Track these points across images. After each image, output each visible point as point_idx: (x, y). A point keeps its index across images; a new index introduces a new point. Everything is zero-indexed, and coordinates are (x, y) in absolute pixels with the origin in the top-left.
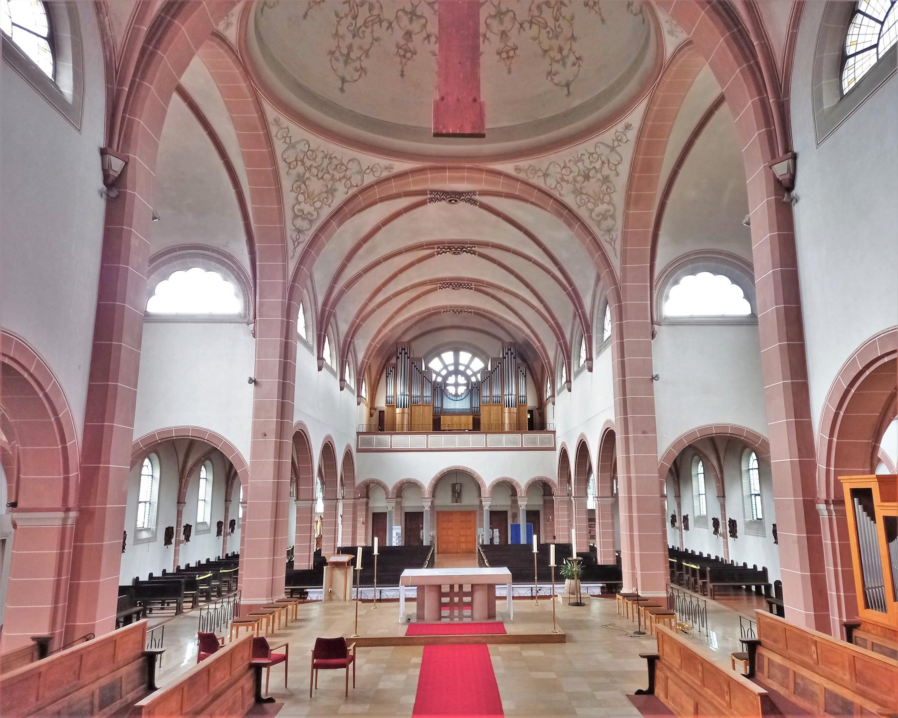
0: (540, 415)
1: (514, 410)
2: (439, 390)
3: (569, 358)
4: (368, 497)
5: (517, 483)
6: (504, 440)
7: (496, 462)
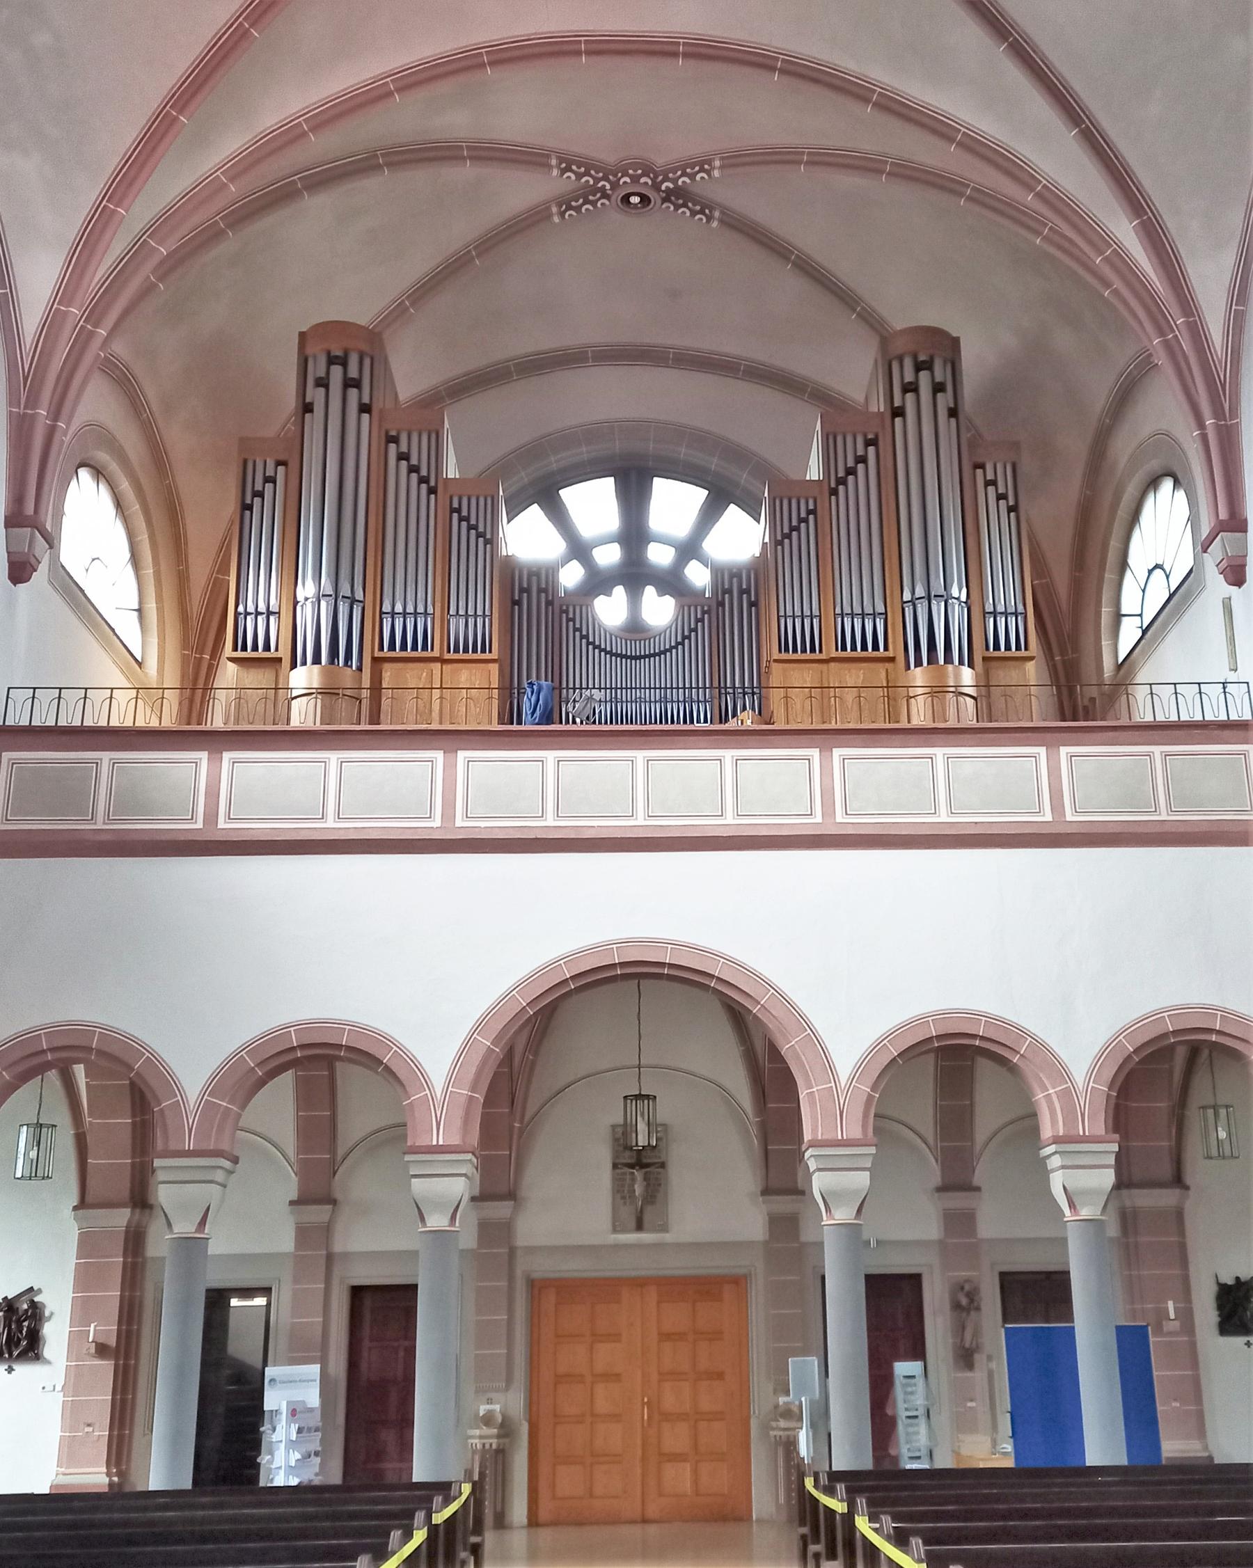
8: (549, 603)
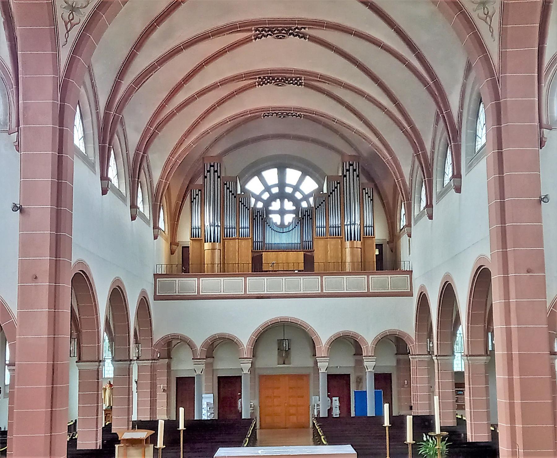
0: (392, 251)
1: (358, 244)
2: (260, 218)
3: (430, 175)
4: (169, 357)
5: (362, 338)
6: (345, 283)
7: (337, 312)
8: (262, 219)
